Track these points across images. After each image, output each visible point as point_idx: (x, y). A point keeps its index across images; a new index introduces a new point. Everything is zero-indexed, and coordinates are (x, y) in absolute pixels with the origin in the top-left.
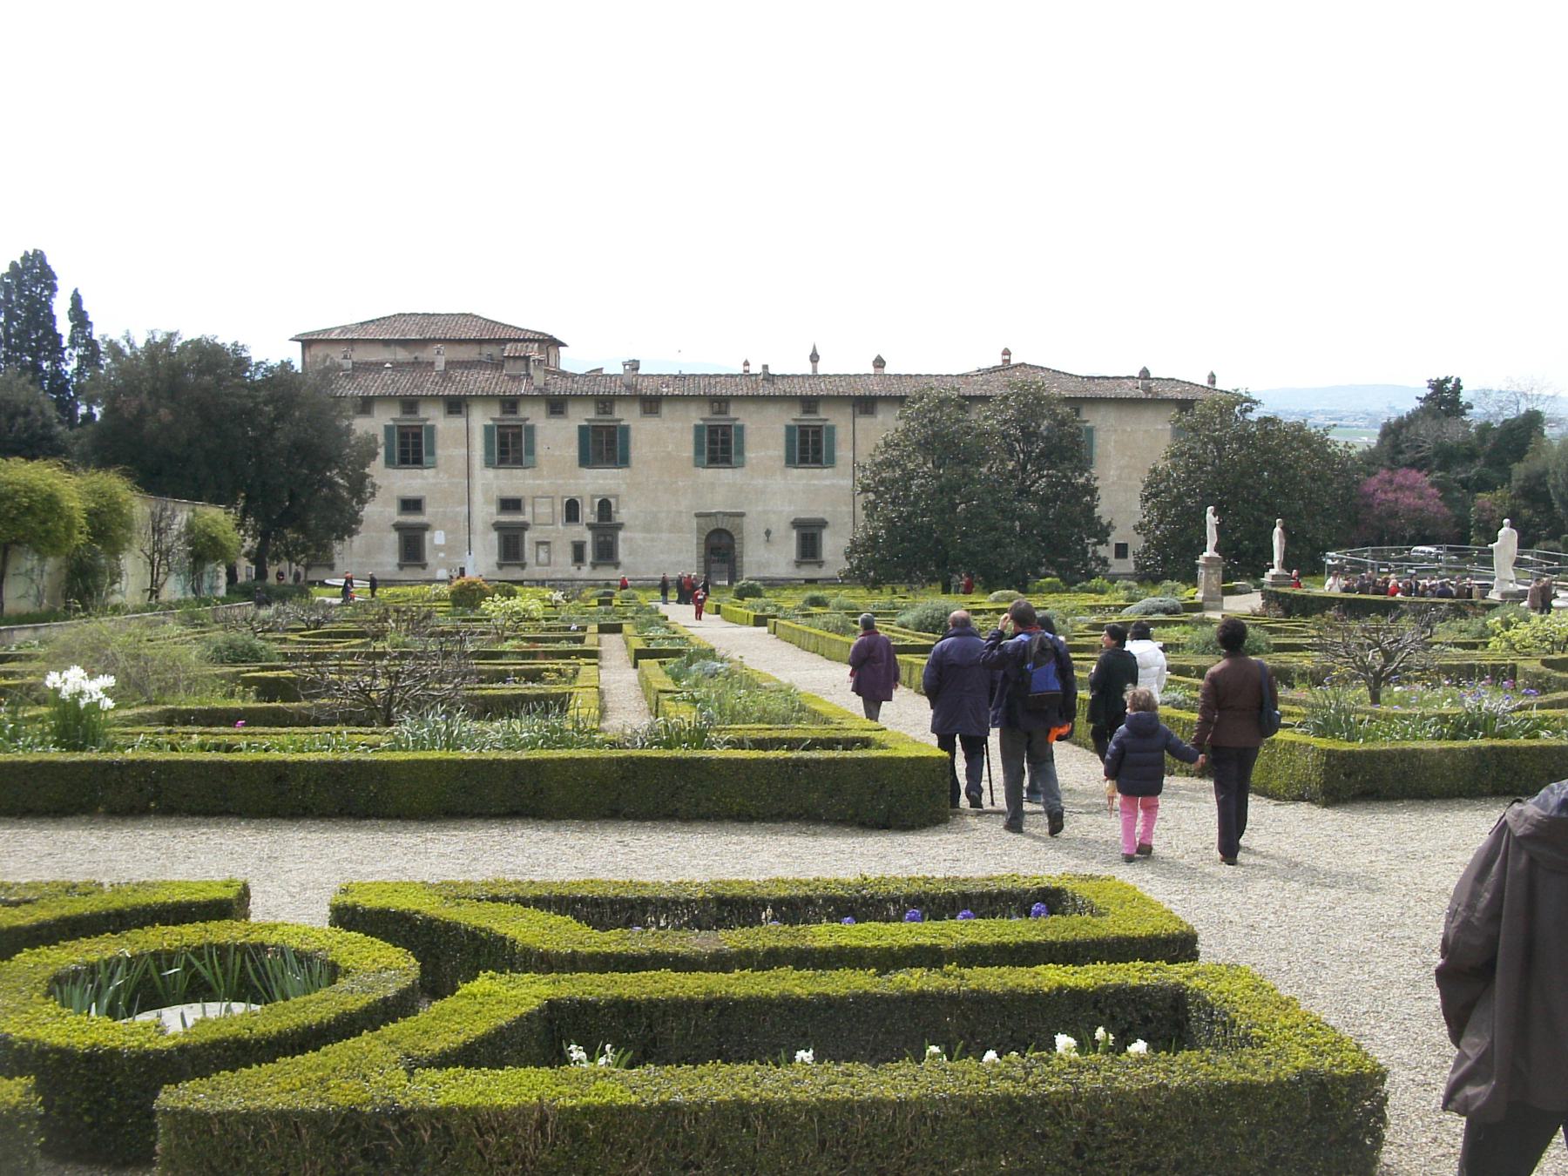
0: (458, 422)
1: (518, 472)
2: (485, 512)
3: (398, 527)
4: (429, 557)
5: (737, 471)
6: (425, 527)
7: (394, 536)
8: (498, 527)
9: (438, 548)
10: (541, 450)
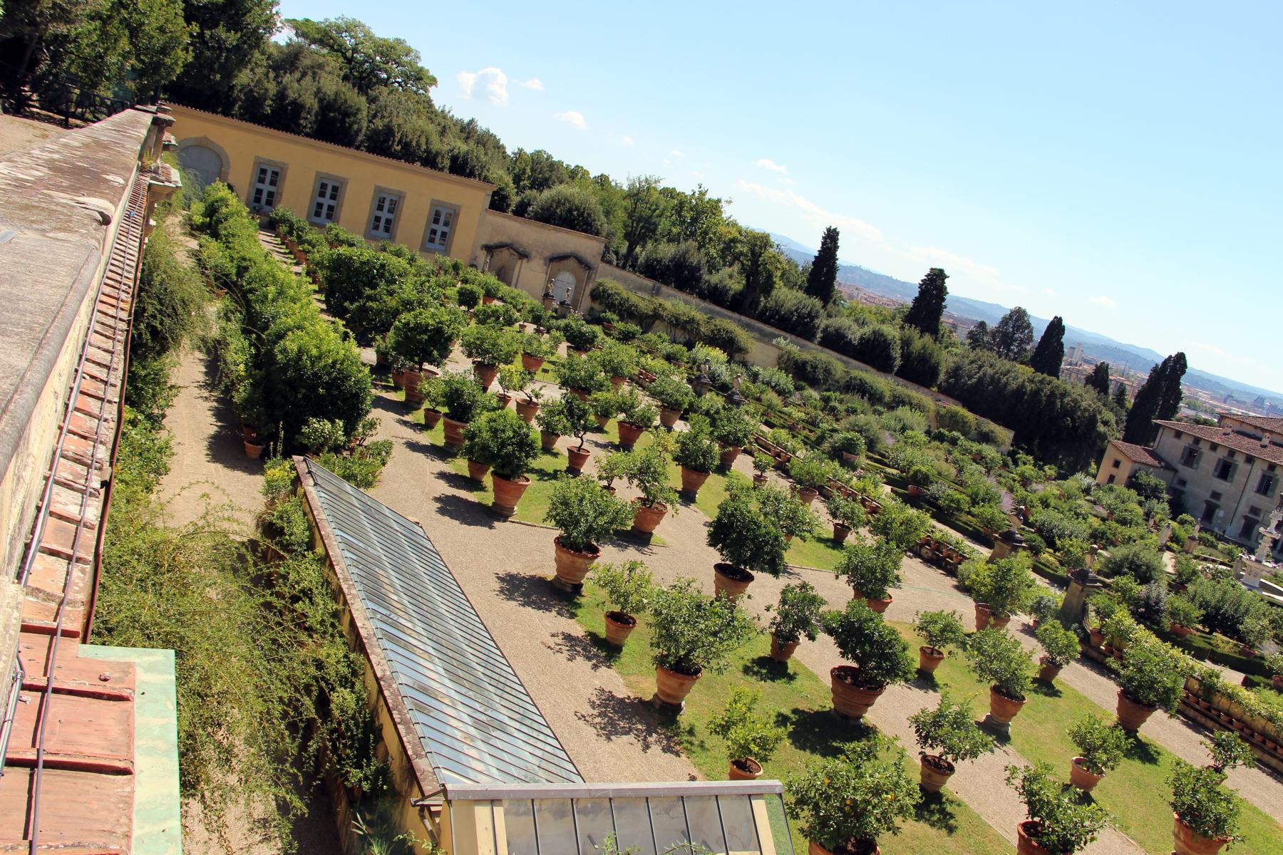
0: (1248, 467)
1: (1263, 497)
2: (1243, 509)
3: (1207, 502)
4: (1214, 521)
6: (1218, 506)
7: (1204, 506)
8: (1245, 517)
9: (1219, 518)
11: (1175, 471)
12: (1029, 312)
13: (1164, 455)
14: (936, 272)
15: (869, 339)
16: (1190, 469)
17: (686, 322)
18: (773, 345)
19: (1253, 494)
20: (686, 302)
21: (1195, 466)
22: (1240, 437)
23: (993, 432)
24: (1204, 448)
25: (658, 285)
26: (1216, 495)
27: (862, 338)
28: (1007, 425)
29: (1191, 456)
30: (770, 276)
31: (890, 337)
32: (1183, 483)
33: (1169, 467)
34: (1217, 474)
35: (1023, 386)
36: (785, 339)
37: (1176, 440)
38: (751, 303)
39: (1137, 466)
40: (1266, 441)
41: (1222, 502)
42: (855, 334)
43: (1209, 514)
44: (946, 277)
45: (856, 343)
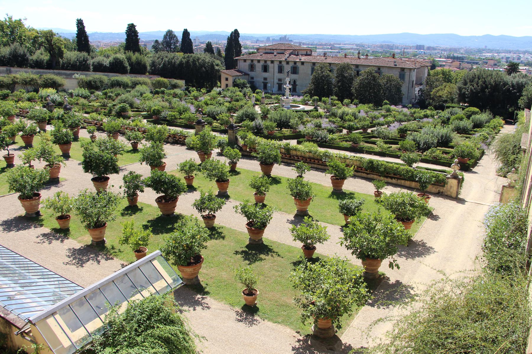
0: (273, 65)
2: (276, 81)
3: (263, 82)
4: (268, 89)
6: (267, 83)
7: (263, 84)
8: (278, 83)
11: (248, 75)
12: (173, 30)
13: (242, 70)
14: (131, 25)
15: (113, 62)
16: (253, 72)
17: (30, 81)
18: (74, 78)
19: (277, 74)
20: (26, 72)
21: (254, 70)
22: (266, 55)
23: (176, 83)
24: (255, 63)
25: (8, 68)
26: (265, 79)
27: (110, 63)
28: (181, 79)
29: (252, 67)
30: (60, 49)
31: (121, 59)
32: (252, 78)
33: (246, 74)
34: (263, 71)
35: (181, 61)
36: (77, 74)
37: (245, 63)
38: (56, 63)
39: (234, 78)
40: (275, 53)
41: (268, 80)
42: (106, 62)
43: (265, 87)
44: (135, 26)
45: (108, 66)
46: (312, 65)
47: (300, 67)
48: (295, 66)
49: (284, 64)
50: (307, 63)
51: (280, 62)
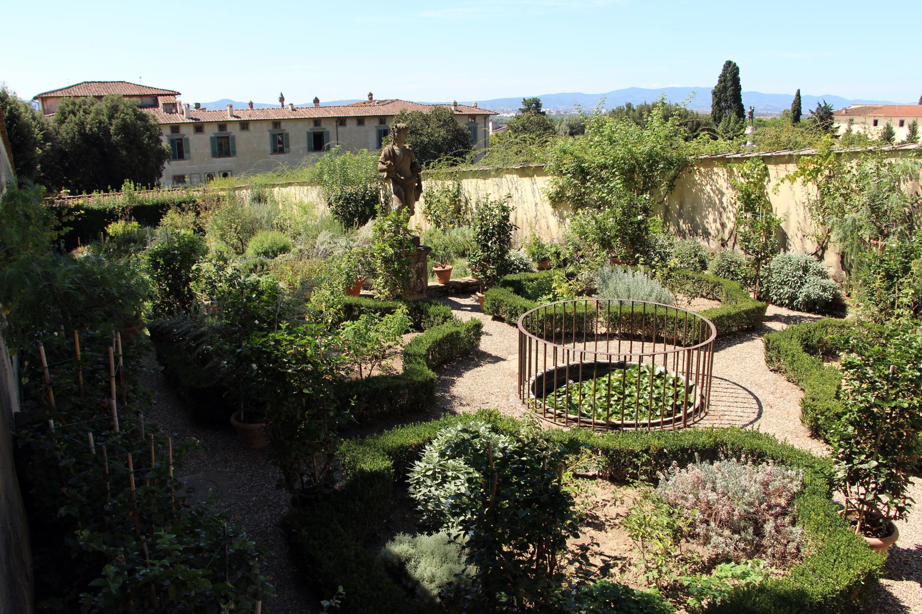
5: (287, 155)
10: (192, 150)
46: (271, 126)
47: (241, 139)
48: (223, 134)
49: (188, 132)
50: (258, 125)
51: (175, 128)
